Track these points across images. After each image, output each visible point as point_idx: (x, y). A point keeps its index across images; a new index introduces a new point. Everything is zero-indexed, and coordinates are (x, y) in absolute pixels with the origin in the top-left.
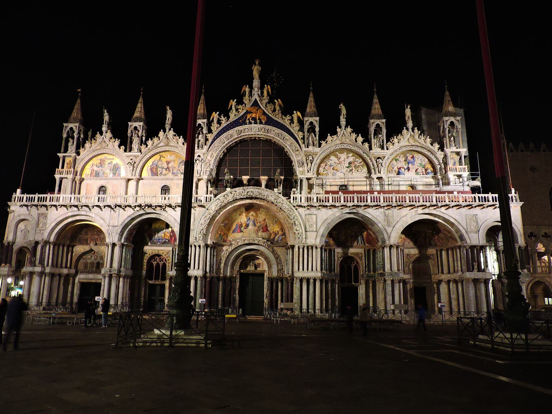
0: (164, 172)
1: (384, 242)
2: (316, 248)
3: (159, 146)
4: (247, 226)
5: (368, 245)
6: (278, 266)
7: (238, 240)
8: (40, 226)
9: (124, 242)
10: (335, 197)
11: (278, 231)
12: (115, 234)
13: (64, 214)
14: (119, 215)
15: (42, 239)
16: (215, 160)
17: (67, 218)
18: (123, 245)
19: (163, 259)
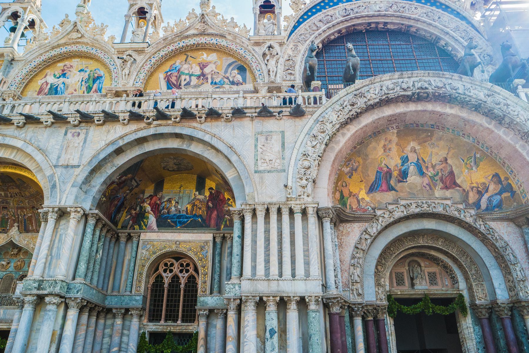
0: (194, 81)
4: (404, 175)
7: (390, 207)
11: (484, 183)
12: (69, 185)
14: (85, 142)
19: (188, 265)
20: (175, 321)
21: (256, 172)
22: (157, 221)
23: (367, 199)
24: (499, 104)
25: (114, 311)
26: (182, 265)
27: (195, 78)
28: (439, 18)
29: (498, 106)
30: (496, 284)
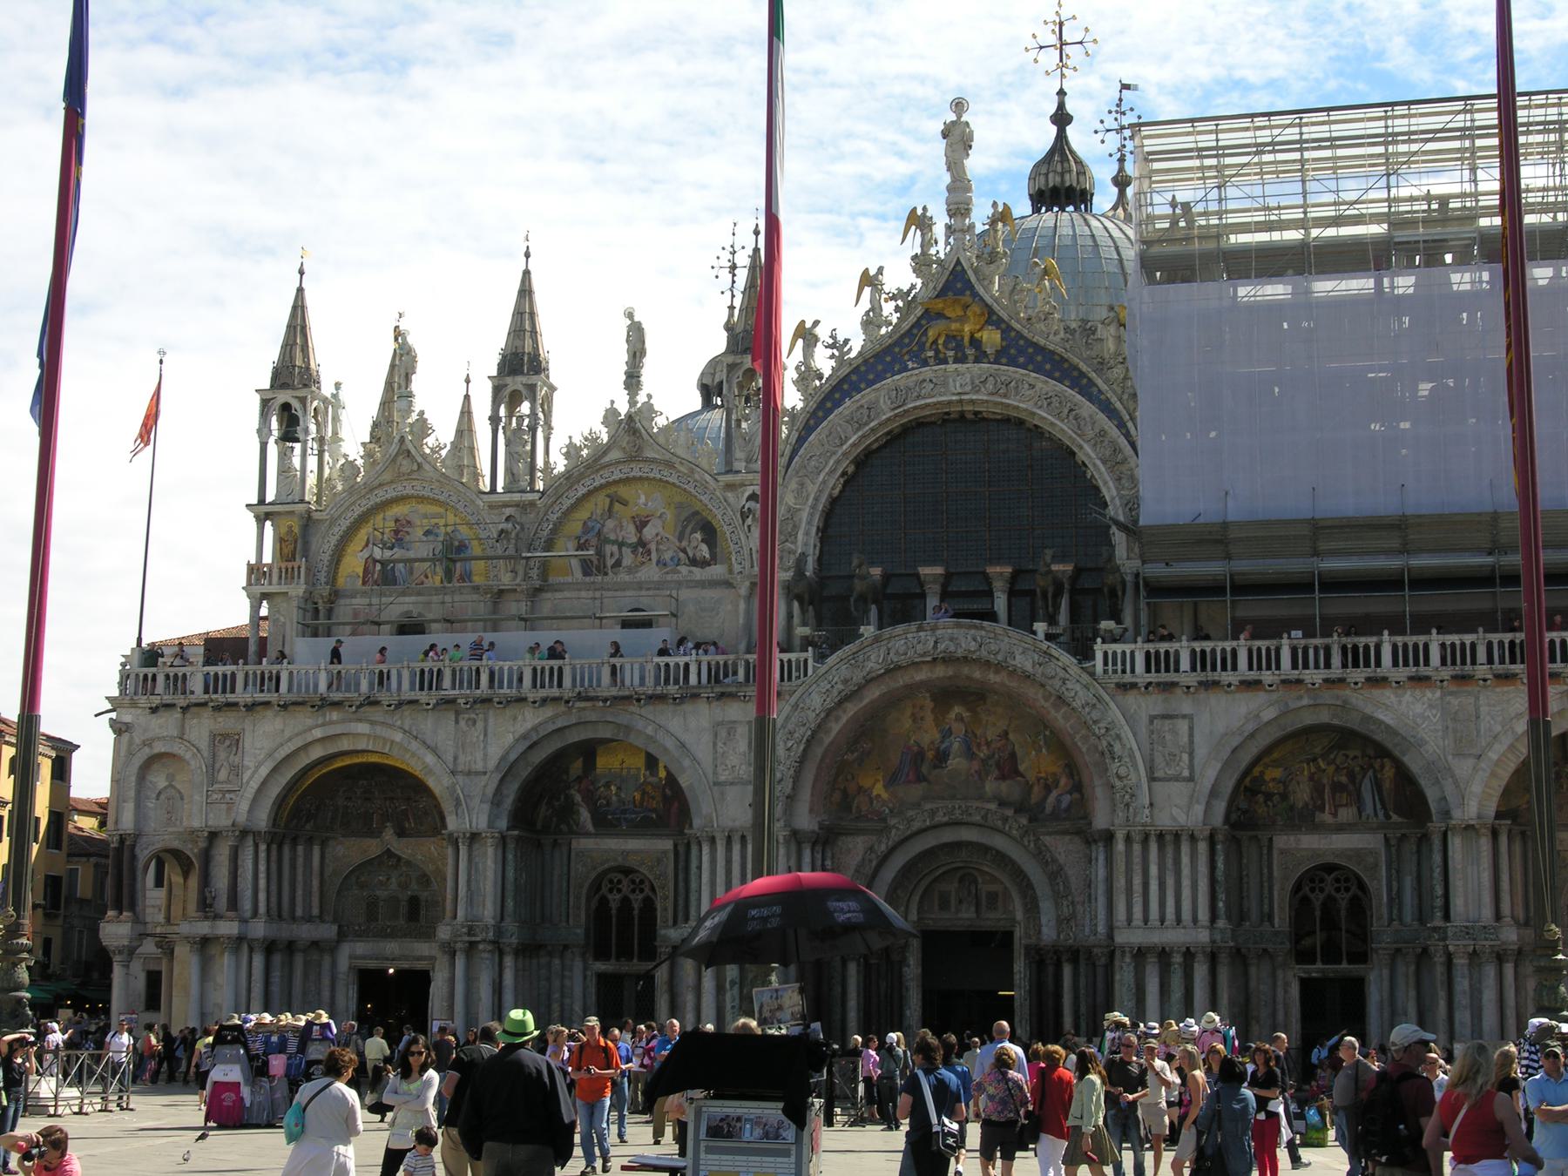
0: (628, 559)
1: (1446, 814)
2: (1193, 838)
3: (606, 459)
4: (942, 757)
5: (1400, 820)
6: (1057, 905)
7: (911, 813)
8: (223, 775)
9: (508, 829)
10: (1259, 650)
11: (1055, 774)
12: (477, 801)
13: (297, 735)
14: (485, 735)
15: (233, 825)
16: (813, 507)
17: (305, 747)
18: (503, 840)
19: (642, 882)
20: (632, 959)
21: (715, 784)
22: (592, 818)
23: (885, 796)
24: (1052, 677)
25: (549, 948)
26: (633, 882)
27: (629, 550)
28: (1071, 410)
29: (1050, 682)
30: (1044, 920)
